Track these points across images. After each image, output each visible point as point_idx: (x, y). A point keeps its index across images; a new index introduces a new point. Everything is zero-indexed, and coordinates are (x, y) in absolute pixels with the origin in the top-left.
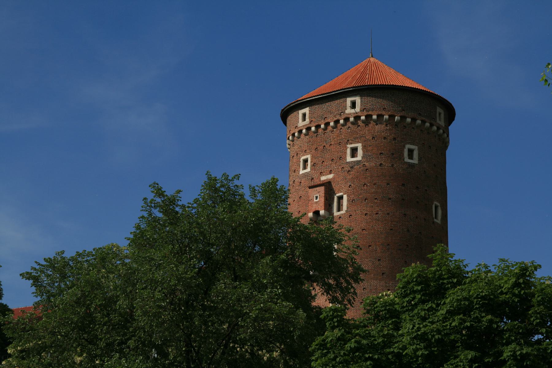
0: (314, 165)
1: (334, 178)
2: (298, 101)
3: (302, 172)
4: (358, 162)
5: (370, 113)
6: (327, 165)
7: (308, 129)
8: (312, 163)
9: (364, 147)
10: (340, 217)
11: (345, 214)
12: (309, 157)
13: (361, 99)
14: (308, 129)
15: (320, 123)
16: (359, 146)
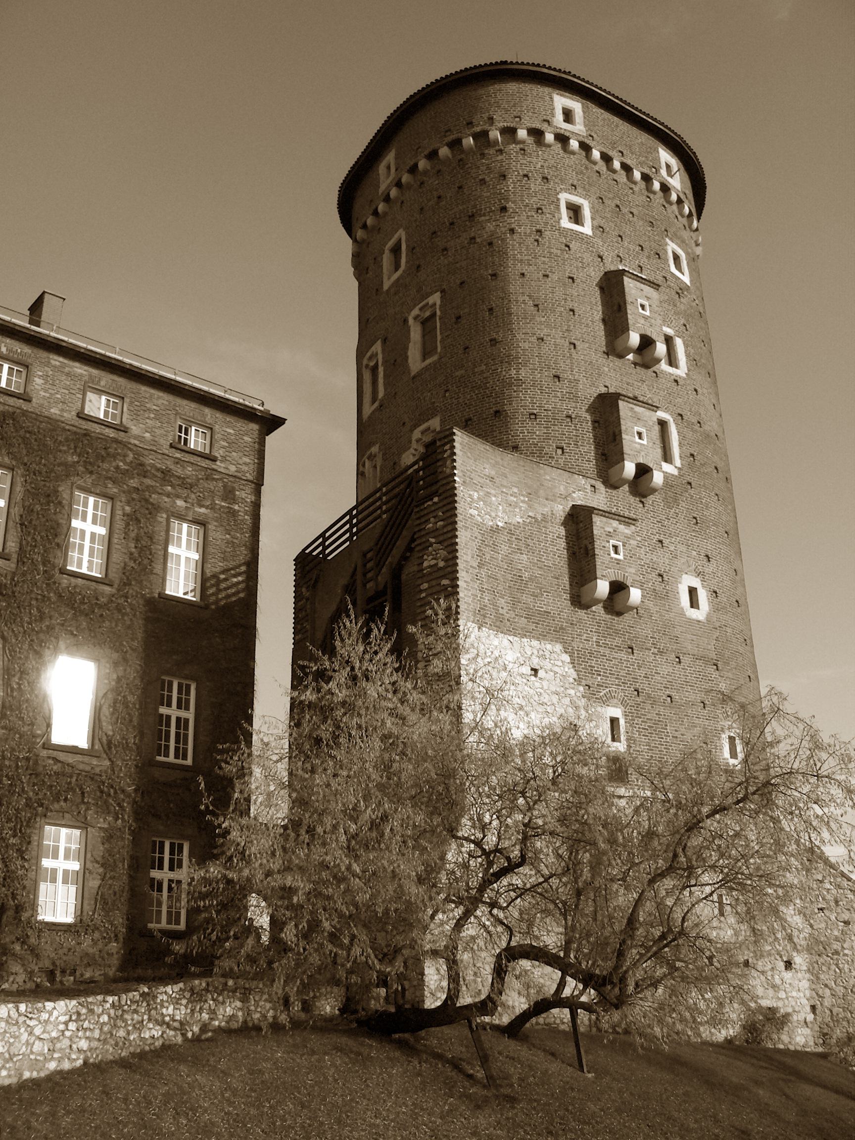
0: (599, 229)
7: (586, 148)
8: (596, 224)
11: (684, 379)
14: (586, 148)
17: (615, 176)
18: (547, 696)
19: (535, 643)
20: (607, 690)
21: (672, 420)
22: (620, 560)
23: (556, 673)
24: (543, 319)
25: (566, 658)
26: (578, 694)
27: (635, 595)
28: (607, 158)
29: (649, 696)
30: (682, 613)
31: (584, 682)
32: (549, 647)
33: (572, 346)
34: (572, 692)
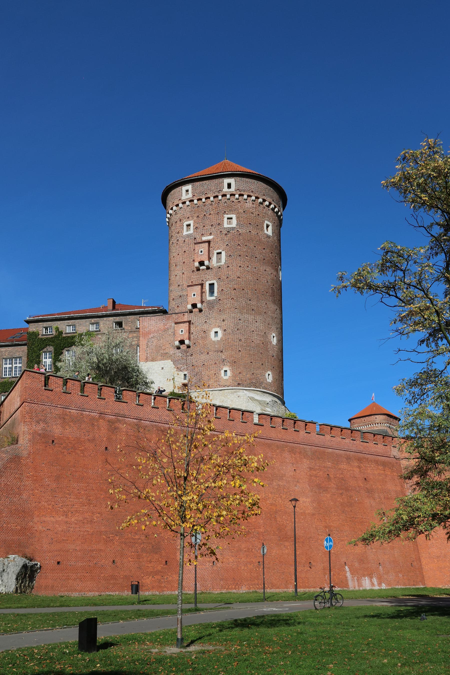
1: (213, 239)
2: (183, 179)
3: (185, 233)
4: (233, 228)
5: (242, 193)
6: (207, 229)
9: (238, 218)
10: (220, 267)
12: (191, 222)
13: (235, 181)
15: (201, 198)
16: (234, 216)
19: (163, 361)
25: (172, 362)
32: (166, 361)
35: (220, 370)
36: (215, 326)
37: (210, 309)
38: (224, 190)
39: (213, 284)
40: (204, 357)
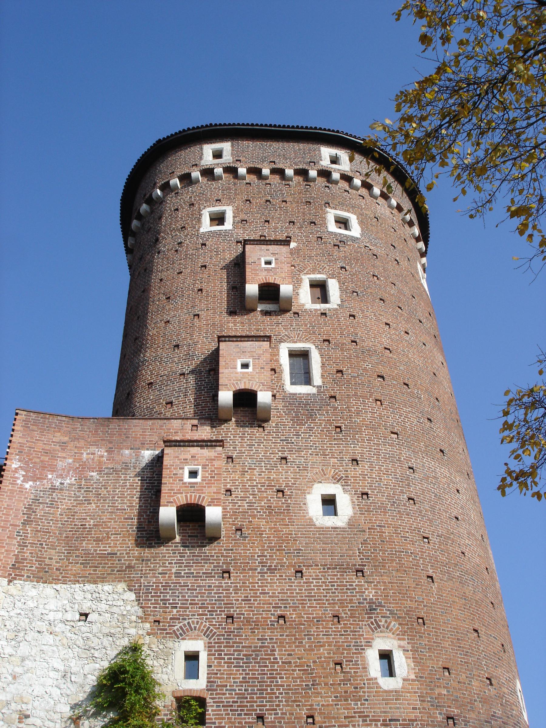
4: (354, 239)
8: (237, 219)
9: (361, 223)
10: (322, 314)
17: (268, 181)
18: (96, 640)
19: (89, 587)
20: (186, 622)
21: (314, 347)
22: (196, 483)
23: (112, 613)
24: (172, 306)
25: (132, 596)
26: (140, 632)
27: (213, 514)
28: (255, 171)
29: (249, 621)
30: (310, 523)
31: (152, 618)
32: (107, 587)
33: (196, 317)
34: (133, 631)
35: (360, 650)
36: (322, 478)
37: (297, 420)
38: (322, 163)
39: (304, 355)
40: (277, 586)
